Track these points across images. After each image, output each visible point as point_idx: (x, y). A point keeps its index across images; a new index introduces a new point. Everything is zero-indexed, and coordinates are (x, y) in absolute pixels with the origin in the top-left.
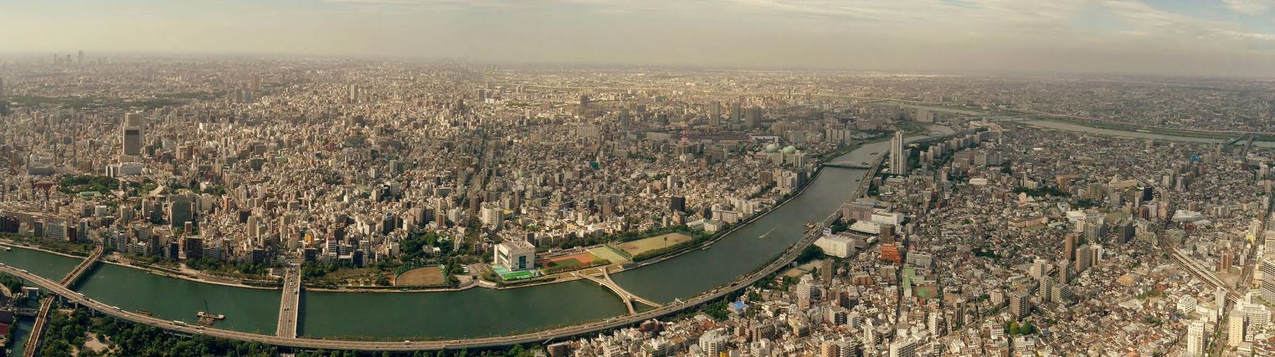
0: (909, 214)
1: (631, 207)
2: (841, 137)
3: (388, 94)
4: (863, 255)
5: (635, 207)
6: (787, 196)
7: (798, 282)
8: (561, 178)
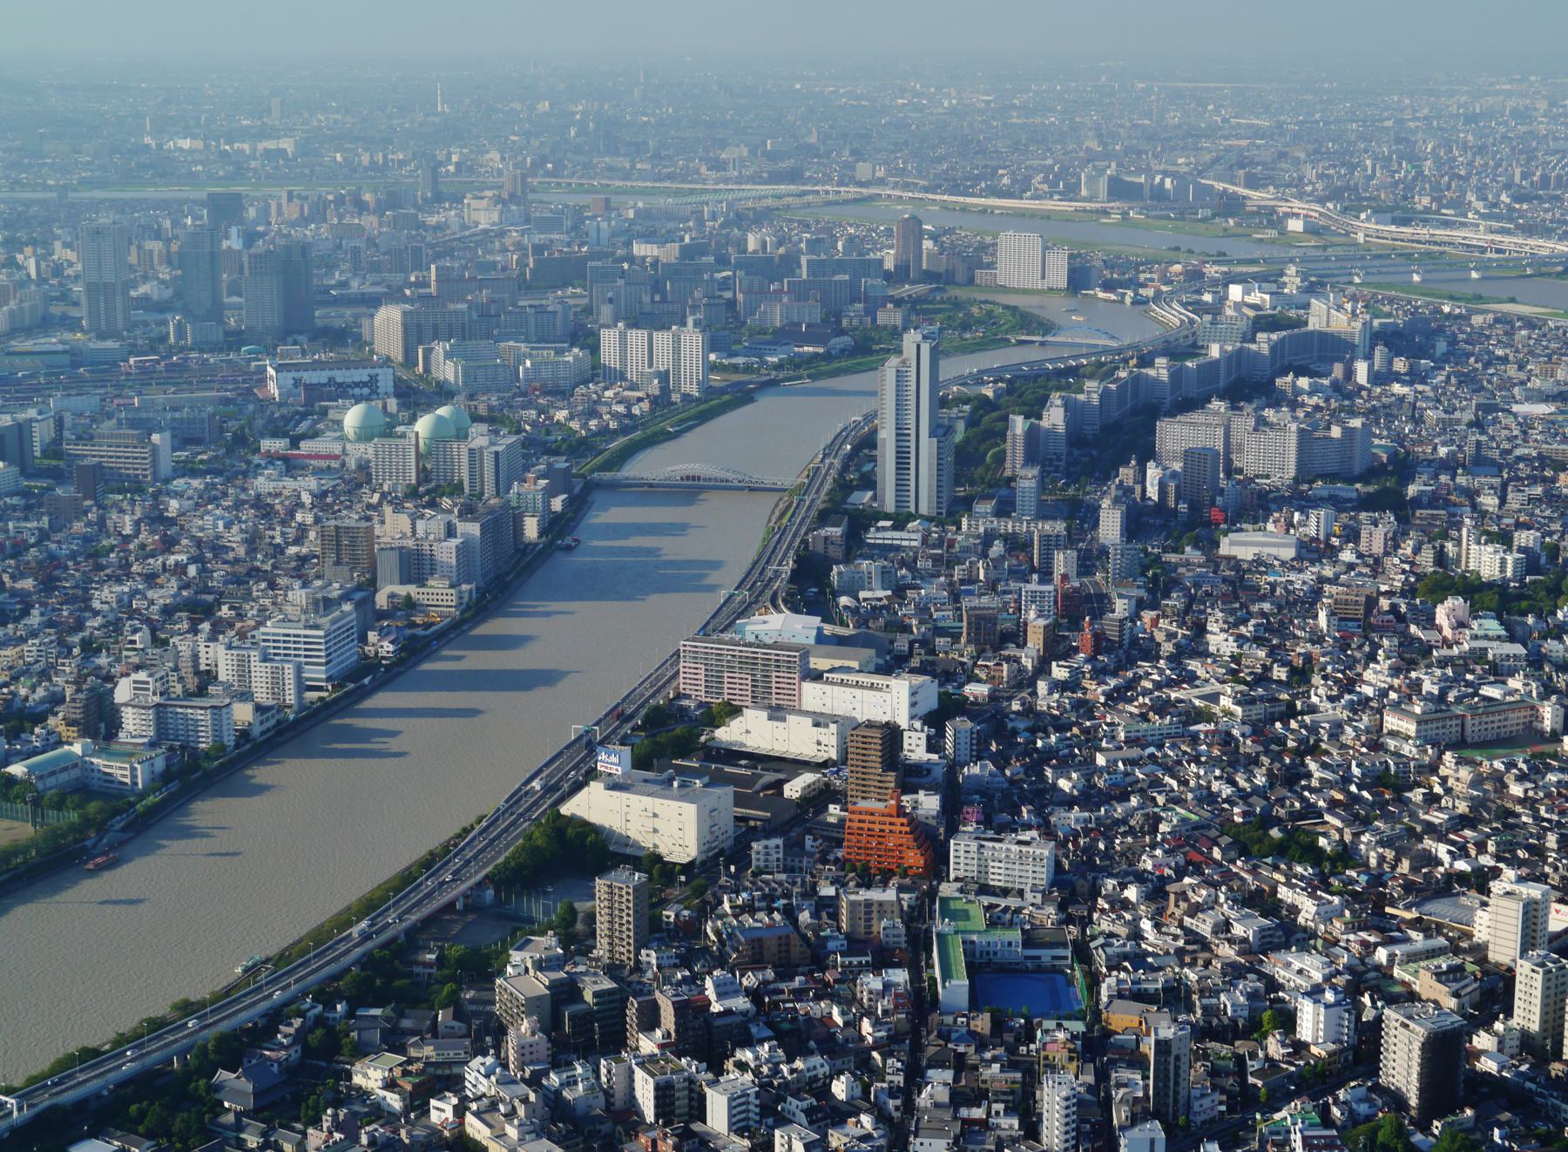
7: (501, 972)
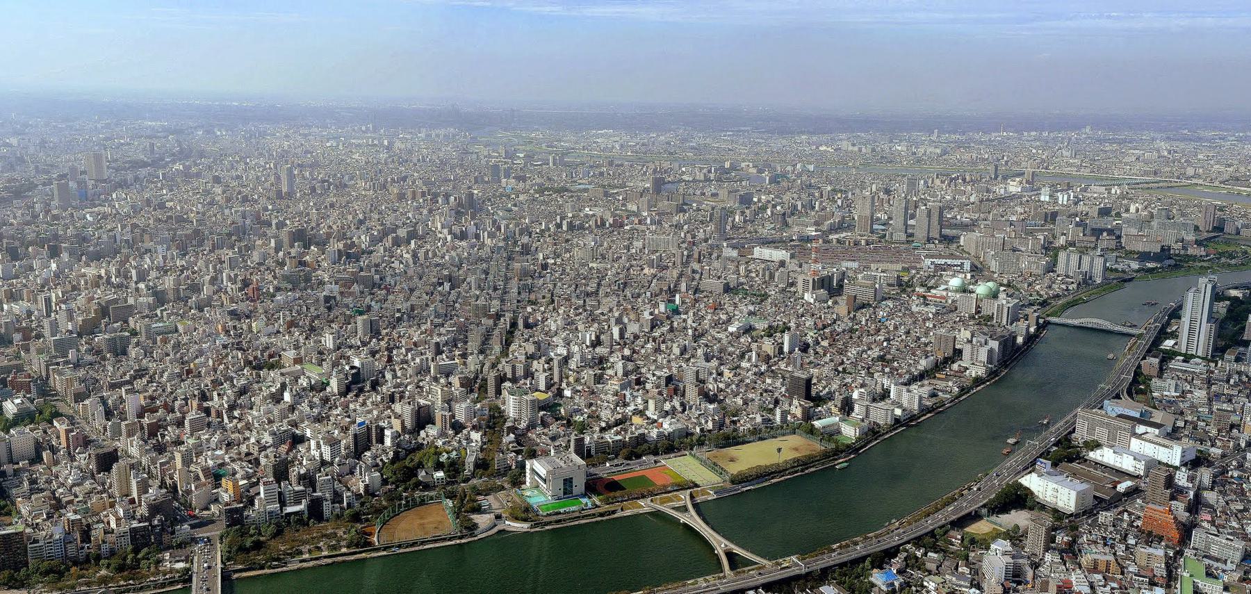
1: (728, 385)
3: (346, 178)
4: (1105, 517)
5: (734, 386)
6: (978, 381)
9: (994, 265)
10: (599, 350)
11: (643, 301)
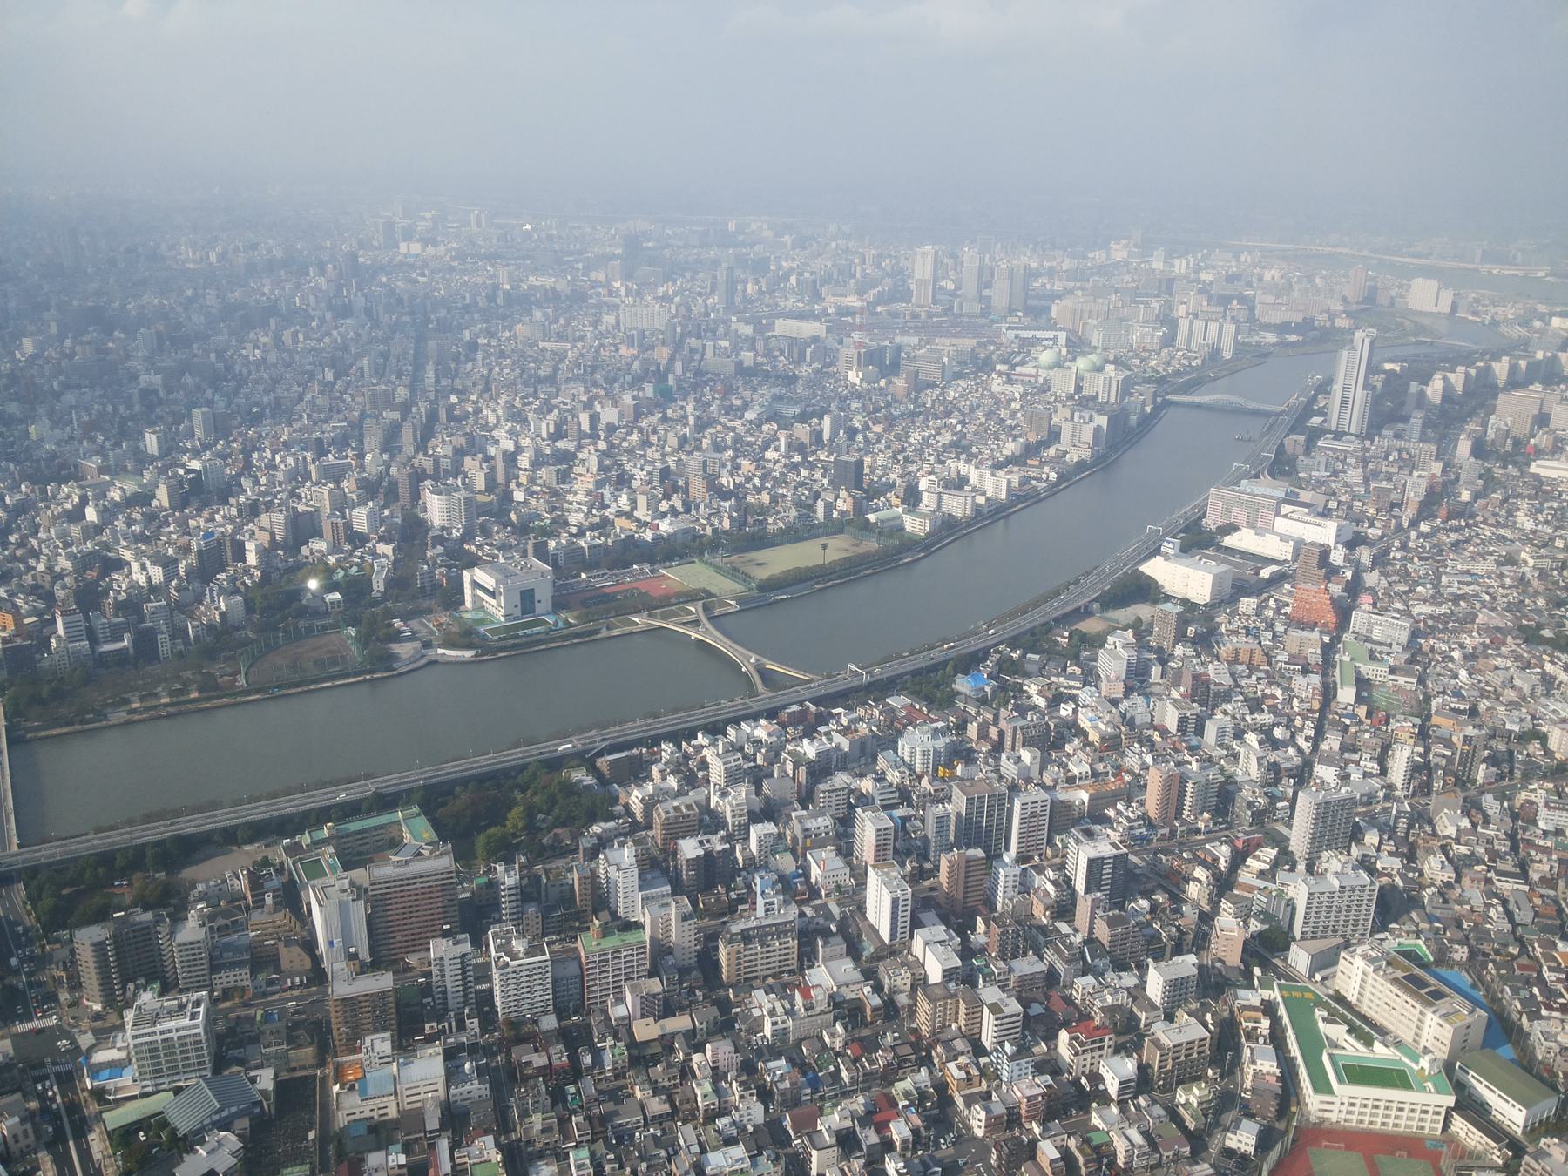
0: (1366, 525)
2: (1212, 337)
4: (1247, 604)
5: (756, 480)
6: (1081, 465)
7: (1102, 646)
8: (594, 419)
9: (1096, 338)
10: (560, 444)
11: (622, 387)
